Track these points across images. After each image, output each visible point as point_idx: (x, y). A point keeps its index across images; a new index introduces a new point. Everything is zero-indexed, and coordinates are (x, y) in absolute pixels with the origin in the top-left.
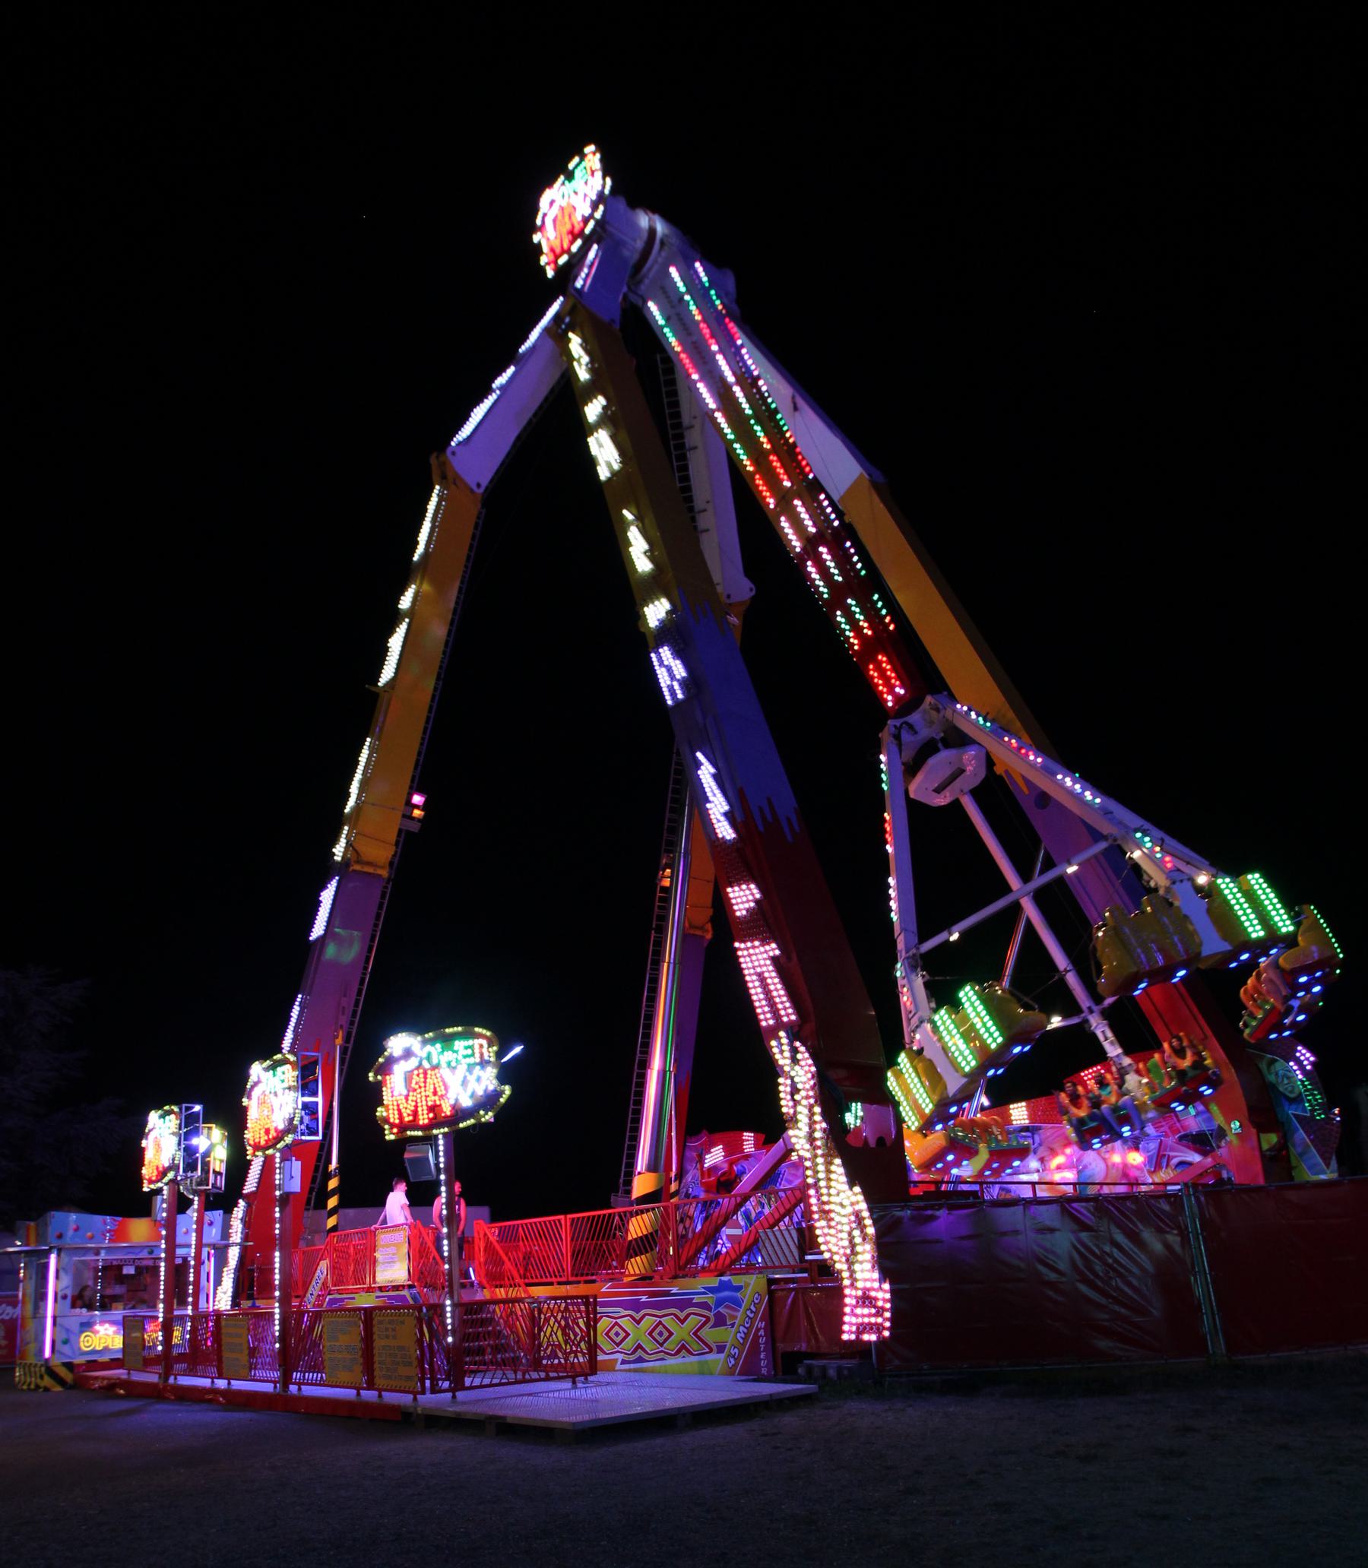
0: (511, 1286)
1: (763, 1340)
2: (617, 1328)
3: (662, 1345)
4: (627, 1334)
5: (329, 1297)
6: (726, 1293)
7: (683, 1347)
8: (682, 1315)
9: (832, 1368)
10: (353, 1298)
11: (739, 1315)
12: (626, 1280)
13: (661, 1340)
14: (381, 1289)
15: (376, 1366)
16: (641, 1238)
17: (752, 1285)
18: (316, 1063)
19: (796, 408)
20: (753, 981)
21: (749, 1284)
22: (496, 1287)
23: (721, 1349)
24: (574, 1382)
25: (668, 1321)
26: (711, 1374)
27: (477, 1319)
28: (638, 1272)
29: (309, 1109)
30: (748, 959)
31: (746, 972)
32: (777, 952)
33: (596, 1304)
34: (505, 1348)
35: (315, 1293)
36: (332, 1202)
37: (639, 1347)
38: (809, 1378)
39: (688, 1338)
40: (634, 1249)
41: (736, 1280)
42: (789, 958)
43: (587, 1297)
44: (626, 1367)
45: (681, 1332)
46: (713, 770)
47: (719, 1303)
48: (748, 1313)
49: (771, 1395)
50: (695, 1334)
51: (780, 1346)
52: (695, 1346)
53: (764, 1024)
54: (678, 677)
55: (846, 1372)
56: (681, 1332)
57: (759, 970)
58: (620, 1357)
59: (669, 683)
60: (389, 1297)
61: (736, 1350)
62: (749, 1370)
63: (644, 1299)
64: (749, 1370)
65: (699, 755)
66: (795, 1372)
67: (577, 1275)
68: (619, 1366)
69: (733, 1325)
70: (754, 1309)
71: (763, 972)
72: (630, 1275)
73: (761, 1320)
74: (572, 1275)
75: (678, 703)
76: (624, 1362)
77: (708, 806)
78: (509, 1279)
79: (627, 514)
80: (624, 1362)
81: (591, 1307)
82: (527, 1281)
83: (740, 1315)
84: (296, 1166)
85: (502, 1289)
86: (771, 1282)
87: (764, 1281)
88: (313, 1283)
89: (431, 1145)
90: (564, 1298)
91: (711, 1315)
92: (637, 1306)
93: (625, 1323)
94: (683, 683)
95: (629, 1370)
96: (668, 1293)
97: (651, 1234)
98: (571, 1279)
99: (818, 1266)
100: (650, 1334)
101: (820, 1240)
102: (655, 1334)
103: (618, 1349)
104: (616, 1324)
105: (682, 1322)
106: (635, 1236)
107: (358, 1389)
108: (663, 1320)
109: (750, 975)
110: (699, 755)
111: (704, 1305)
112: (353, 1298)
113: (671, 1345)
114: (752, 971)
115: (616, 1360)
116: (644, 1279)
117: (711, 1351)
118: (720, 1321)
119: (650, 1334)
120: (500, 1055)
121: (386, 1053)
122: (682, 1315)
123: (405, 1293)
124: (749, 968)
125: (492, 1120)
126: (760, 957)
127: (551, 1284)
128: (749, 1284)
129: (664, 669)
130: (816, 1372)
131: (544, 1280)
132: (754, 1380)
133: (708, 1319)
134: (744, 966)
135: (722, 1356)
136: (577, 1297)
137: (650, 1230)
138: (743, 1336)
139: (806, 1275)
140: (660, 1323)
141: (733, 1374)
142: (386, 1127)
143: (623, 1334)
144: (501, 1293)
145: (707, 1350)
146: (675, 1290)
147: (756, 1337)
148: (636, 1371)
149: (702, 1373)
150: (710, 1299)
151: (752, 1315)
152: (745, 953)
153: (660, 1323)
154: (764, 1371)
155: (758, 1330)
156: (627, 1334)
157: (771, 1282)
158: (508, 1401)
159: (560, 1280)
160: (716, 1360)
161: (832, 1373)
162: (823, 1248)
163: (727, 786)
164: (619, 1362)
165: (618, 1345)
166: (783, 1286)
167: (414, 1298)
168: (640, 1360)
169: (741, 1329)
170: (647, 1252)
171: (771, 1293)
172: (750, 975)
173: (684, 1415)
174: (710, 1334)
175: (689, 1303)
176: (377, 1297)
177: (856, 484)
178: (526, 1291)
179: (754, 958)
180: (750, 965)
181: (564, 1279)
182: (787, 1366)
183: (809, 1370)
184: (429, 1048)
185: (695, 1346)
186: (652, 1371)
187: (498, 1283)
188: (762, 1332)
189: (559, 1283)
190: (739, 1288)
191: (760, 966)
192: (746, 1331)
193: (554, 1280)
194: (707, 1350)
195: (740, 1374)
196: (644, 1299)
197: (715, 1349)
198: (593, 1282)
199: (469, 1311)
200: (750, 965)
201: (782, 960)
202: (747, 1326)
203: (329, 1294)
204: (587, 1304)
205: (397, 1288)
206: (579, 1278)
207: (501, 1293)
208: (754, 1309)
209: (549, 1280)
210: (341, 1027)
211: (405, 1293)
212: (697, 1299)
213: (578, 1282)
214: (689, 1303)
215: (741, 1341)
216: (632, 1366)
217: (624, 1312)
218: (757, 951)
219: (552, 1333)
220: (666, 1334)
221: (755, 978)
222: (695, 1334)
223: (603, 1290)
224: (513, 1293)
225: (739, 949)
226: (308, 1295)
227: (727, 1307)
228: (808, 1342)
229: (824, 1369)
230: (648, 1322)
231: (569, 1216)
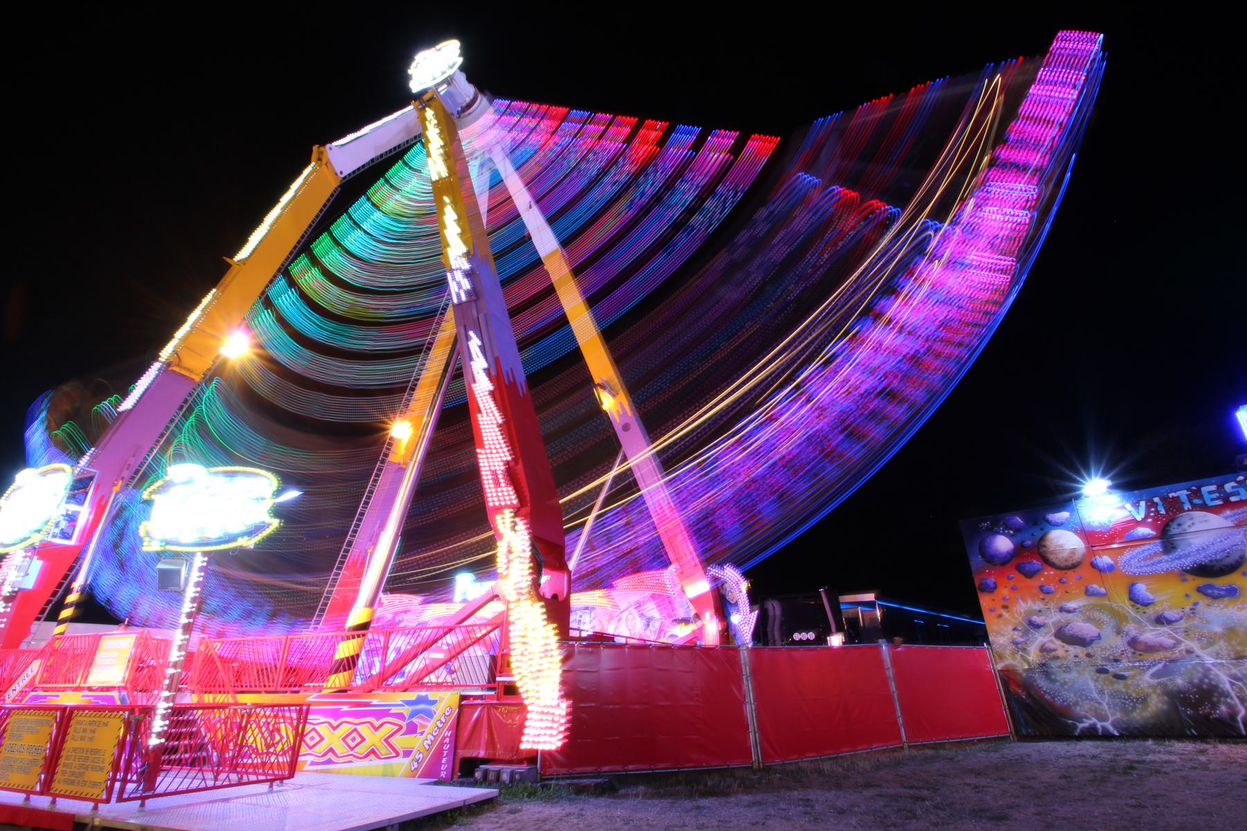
0: (220, 692)
1: (446, 747)
2: (313, 733)
3: (352, 749)
4: (322, 739)
5: (33, 693)
6: (421, 706)
7: (373, 752)
8: (377, 724)
9: (506, 771)
10: (58, 696)
11: (430, 724)
12: (324, 692)
13: (352, 744)
14: (90, 689)
15: (59, 769)
16: (347, 658)
17: (446, 702)
18: (91, 478)
19: (531, 207)
20: (487, 475)
21: (443, 699)
22: (206, 693)
23: (407, 753)
24: (271, 786)
25: (364, 729)
26: (393, 776)
27: (183, 721)
28: (338, 685)
29: (72, 519)
30: (485, 460)
31: (483, 469)
32: (509, 458)
33: (308, 712)
34: (202, 747)
35: (18, 689)
36: (66, 613)
37: (331, 750)
38: (485, 781)
39: (378, 744)
40: (344, 667)
41: (432, 695)
42: (516, 464)
43: (301, 705)
44: (315, 767)
45: (373, 738)
46: (479, 343)
47: (414, 714)
48: (438, 723)
49: (465, 801)
50: (386, 740)
51: (459, 751)
52: (383, 750)
53: (491, 504)
54: (464, 288)
55: (517, 777)
56: (373, 738)
57: (493, 468)
58: (310, 759)
59: (457, 290)
60: (96, 697)
61: (421, 755)
62: (431, 774)
63: (345, 708)
64: (431, 774)
65: (471, 333)
66: (472, 774)
67: (285, 686)
68: (307, 767)
69: (422, 733)
70: (443, 720)
71: (496, 470)
72: (331, 688)
73: (448, 730)
74: (281, 686)
75: (460, 304)
76: (313, 763)
77: (472, 363)
78: (219, 686)
79: (446, 199)
80: (313, 763)
81: (304, 713)
82: (236, 689)
83: (430, 726)
84: (37, 565)
85: (211, 695)
86: (463, 698)
87: (457, 697)
88: (20, 679)
89: (187, 561)
90: (273, 706)
91: (404, 724)
92: (336, 714)
93: (323, 729)
94: (468, 293)
95: (316, 771)
96: (368, 704)
97: (352, 657)
98: (278, 689)
99: (505, 686)
100: (344, 739)
101: (513, 665)
102: (348, 740)
103: (310, 751)
104: (314, 729)
105: (376, 729)
106: (342, 656)
107: (29, 793)
108: (359, 728)
109: (486, 471)
110: (471, 333)
111: (400, 716)
112: (58, 696)
113: (362, 749)
114: (487, 468)
115: (306, 761)
116: (342, 691)
117: (398, 755)
118: (412, 729)
119: (344, 739)
120: (278, 493)
121: (167, 478)
122: (377, 724)
123: (115, 694)
124: (485, 466)
125: (252, 547)
126: (495, 460)
127: (259, 692)
128: (443, 699)
129: (454, 283)
130: (491, 776)
131: (254, 689)
132: (435, 783)
133: (401, 727)
134: (481, 464)
135: (407, 760)
136: (289, 705)
137: (352, 654)
138: (429, 742)
139: (493, 693)
140: (355, 730)
141: (414, 777)
142: (147, 539)
143: (318, 739)
144: (208, 698)
145: (394, 755)
146: (375, 702)
147: (442, 744)
148: (322, 771)
149: (384, 775)
150: (406, 710)
151: (440, 726)
152: (484, 456)
153: (355, 730)
154: (443, 774)
155: (444, 738)
156: (322, 739)
157: (463, 698)
158: (203, 808)
159: (267, 689)
160: (402, 764)
161: (505, 777)
162: (514, 672)
163: (489, 353)
164: (309, 763)
165: (311, 748)
166: (472, 701)
167: (123, 699)
168: (330, 762)
169: (430, 737)
170: (345, 670)
171: (461, 707)
172: (486, 471)
173: (392, 826)
174: (400, 741)
175: (386, 713)
176: (83, 696)
177: (554, 253)
178: (234, 698)
179: (490, 460)
180: (486, 464)
181: (272, 689)
182: (466, 770)
183: (486, 773)
184: (213, 478)
185: (383, 750)
186: (338, 772)
187: (209, 689)
188: (447, 740)
189: (266, 692)
190: (434, 702)
191: (494, 466)
192: (433, 739)
193: (263, 689)
194: (394, 755)
195: (422, 776)
196: (345, 708)
197: (401, 753)
198: (297, 692)
199: (178, 714)
200: (486, 464)
201: (512, 464)
202: (435, 734)
203: (33, 691)
204: (300, 712)
205: (108, 689)
206: (286, 689)
207: (208, 698)
208: (443, 720)
209: (258, 689)
210: (123, 478)
211: (115, 694)
212: (394, 710)
213: (286, 692)
214: (386, 713)
215: (427, 747)
216: (320, 767)
217: (322, 719)
218: (493, 456)
219: (254, 737)
220: (359, 739)
221: (488, 473)
222: (386, 740)
223: (308, 699)
224: (221, 698)
225: (481, 453)
226: (10, 690)
227: (420, 718)
228: (487, 749)
229: (499, 773)
230: (345, 728)
231: (290, 637)
